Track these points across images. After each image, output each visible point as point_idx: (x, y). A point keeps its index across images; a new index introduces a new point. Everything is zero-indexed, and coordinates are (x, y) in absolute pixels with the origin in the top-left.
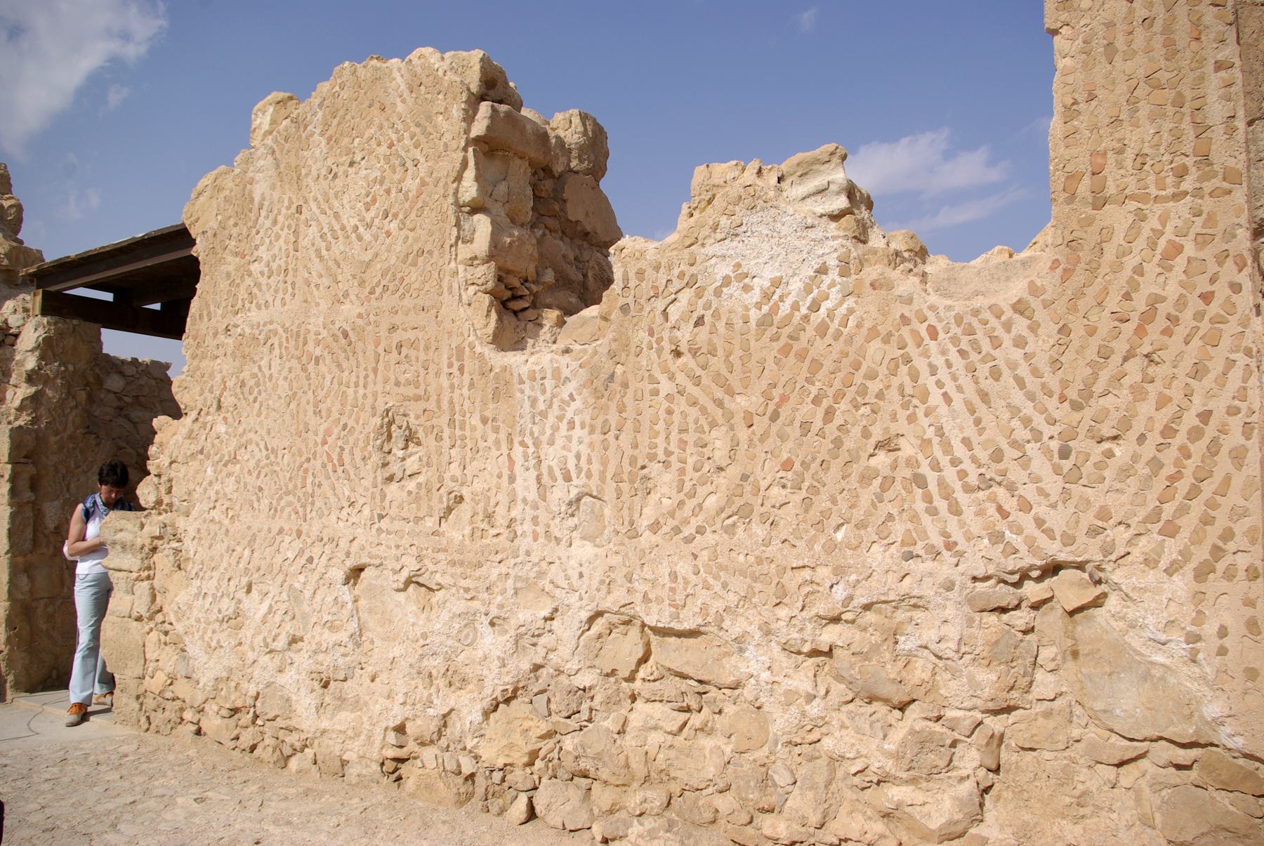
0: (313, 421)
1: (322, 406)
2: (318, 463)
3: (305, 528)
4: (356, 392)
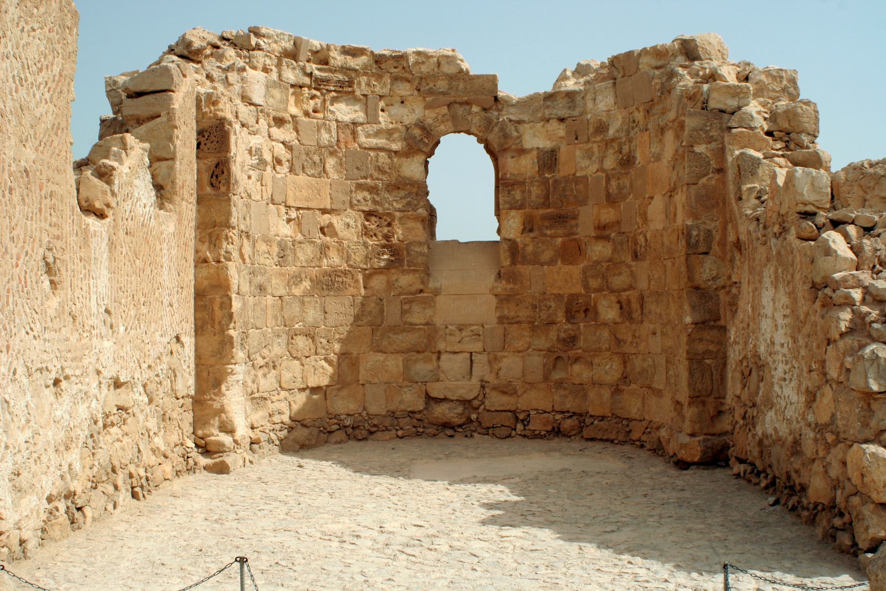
0: (10, 245)
1: (15, 233)
2: (15, 283)
3: (11, 343)
4: (32, 225)
